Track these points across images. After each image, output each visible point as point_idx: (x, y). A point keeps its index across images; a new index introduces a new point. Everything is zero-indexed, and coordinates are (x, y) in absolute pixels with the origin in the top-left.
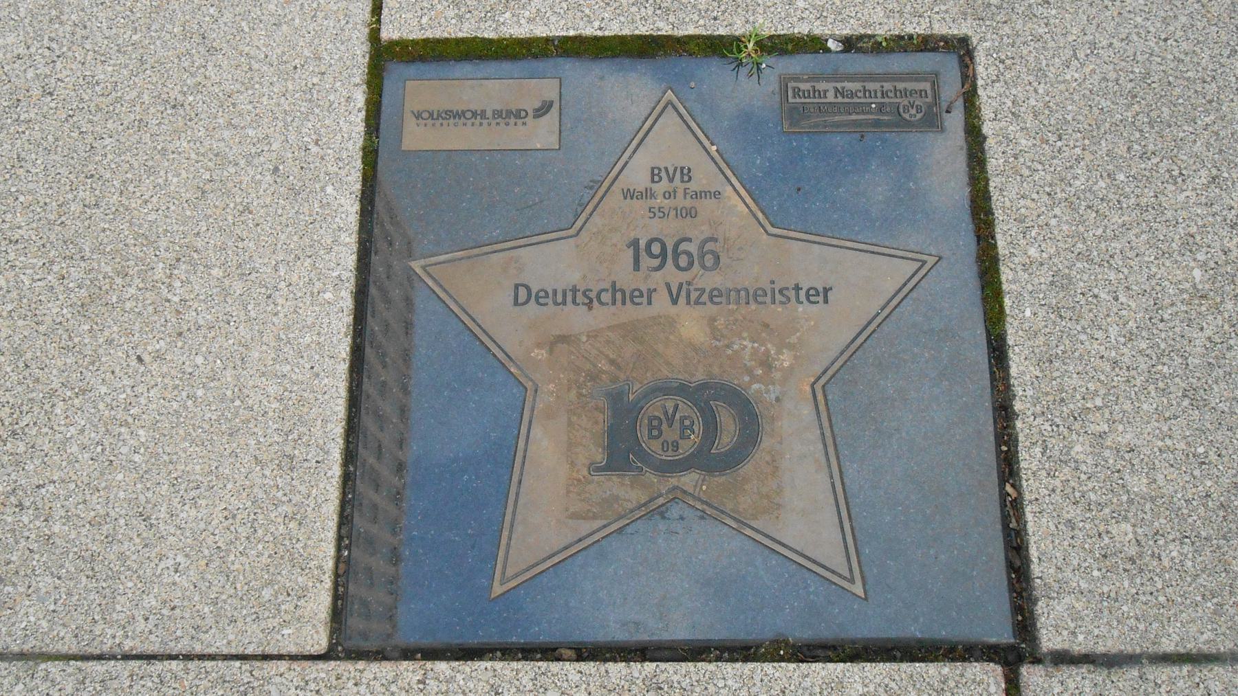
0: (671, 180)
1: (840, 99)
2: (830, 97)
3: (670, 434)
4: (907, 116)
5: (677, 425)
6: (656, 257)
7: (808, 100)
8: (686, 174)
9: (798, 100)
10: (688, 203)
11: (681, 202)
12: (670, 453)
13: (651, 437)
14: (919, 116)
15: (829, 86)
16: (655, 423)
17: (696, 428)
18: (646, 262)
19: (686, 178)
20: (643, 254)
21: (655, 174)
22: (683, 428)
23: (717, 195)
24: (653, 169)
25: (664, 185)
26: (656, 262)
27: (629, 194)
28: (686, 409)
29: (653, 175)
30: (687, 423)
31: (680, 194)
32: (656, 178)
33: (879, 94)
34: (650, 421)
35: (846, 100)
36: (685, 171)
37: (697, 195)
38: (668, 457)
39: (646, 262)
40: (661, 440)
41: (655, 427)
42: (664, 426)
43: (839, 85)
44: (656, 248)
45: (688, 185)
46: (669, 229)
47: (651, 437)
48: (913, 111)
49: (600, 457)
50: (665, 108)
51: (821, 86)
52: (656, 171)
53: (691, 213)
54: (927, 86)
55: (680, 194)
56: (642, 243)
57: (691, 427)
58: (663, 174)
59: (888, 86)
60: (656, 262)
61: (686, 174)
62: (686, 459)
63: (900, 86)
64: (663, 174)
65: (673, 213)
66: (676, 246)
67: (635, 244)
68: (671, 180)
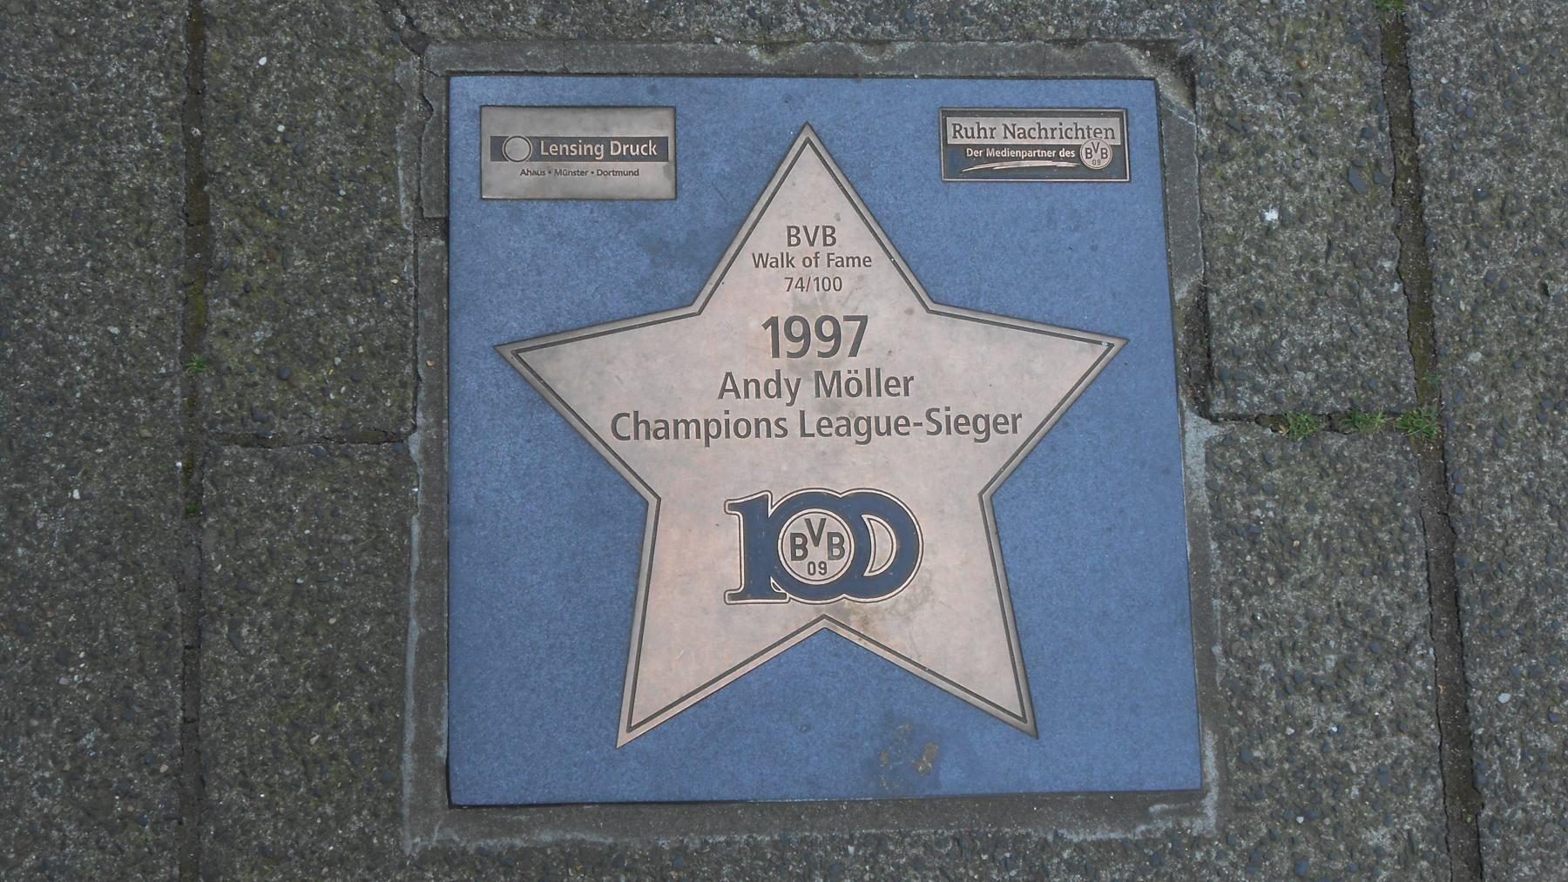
0: (812, 244)
1: (1010, 141)
3: (818, 553)
4: (1088, 163)
6: (796, 340)
9: (958, 141)
11: (822, 271)
12: (817, 576)
13: (794, 557)
14: (1104, 163)
15: (999, 123)
16: (799, 541)
17: (846, 546)
18: (786, 345)
21: (792, 232)
22: (831, 546)
23: (866, 262)
26: (799, 346)
27: (760, 260)
28: (835, 523)
29: (790, 236)
30: (836, 540)
31: (823, 260)
32: (794, 240)
33: (1057, 133)
34: (794, 536)
36: (829, 231)
38: (817, 579)
39: (786, 345)
40: (806, 561)
41: (799, 547)
42: (810, 545)
43: (1008, 121)
44: (797, 329)
47: (794, 557)
48: (1097, 156)
51: (986, 123)
52: (793, 232)
53: (835, 284)
54: (1114, 123)
55: (823, 260)
57: (840, 546)
58: (802, 235)
59: (1068, 123)
60: (799, 346)
61: (829, 234)
63: (1083, 122)
64: (802, 235)
66: (834, 351)
67: (773, 322)
68: (812, 244)
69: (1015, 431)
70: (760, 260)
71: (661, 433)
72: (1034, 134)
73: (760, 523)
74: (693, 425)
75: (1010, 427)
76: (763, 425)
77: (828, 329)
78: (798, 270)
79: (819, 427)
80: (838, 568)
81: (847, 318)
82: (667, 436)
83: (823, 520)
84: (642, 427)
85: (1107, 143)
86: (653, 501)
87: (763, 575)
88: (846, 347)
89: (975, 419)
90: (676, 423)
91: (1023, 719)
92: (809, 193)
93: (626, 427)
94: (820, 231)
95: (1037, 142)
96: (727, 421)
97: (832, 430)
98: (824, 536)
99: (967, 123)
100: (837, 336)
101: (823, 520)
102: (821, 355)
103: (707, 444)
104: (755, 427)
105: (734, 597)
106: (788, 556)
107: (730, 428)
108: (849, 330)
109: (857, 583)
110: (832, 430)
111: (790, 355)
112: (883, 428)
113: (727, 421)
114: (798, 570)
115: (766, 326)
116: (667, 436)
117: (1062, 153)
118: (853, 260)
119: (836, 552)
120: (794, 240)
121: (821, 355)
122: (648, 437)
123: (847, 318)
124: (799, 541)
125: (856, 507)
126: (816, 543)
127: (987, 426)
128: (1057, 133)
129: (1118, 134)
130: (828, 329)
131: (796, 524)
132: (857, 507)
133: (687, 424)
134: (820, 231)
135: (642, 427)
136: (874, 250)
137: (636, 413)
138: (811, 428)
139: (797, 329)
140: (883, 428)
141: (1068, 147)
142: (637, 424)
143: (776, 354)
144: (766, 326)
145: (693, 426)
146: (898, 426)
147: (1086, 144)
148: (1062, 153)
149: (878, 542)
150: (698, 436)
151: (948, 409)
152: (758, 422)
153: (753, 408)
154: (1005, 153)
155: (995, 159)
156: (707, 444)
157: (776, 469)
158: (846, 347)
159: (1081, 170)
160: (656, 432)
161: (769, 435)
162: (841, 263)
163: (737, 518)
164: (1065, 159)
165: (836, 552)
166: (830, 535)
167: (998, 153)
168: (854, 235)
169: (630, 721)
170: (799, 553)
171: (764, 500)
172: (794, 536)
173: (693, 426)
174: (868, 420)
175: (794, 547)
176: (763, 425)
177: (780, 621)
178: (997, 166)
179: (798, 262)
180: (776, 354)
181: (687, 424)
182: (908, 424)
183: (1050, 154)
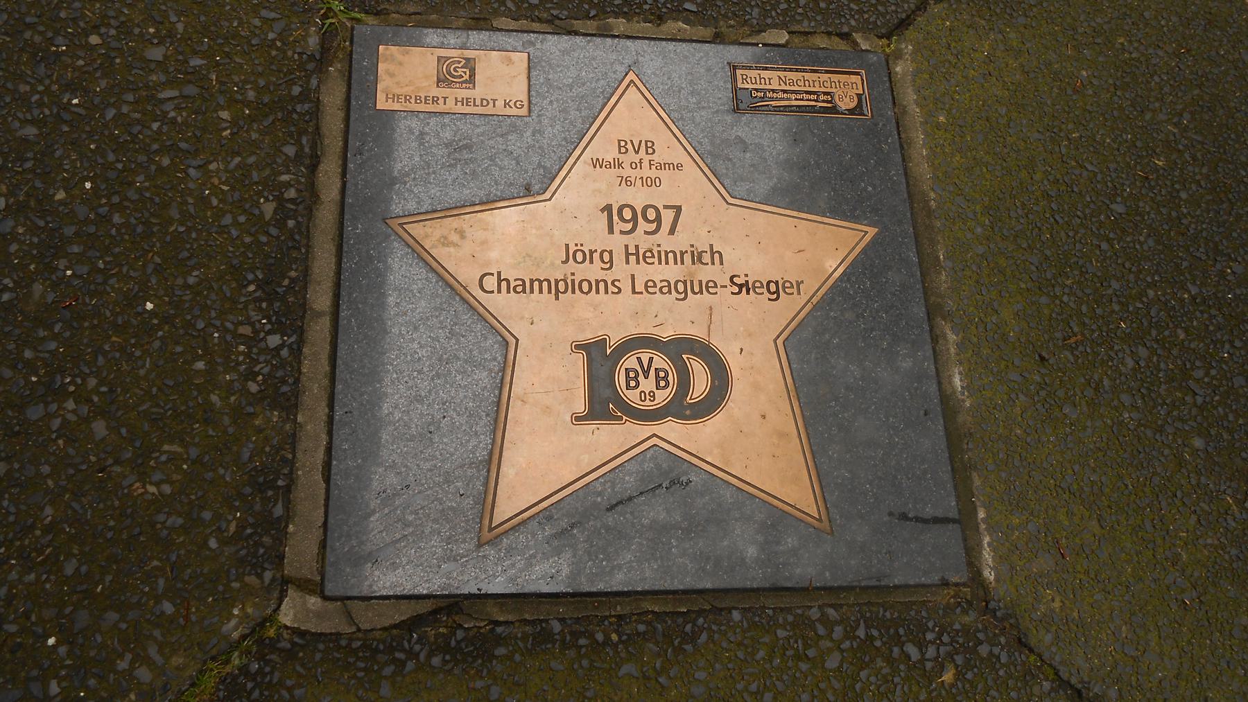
0: (637, 152)
3: (647, 384)
5: (652, 372)
7: (755, 86)
10: (653, 173)
11: (646, 172)
12: (648, 402)
17: (670, 378)
19: (650, 151)
20: (615, 218)
21: (622, 146)
23: (679, 167)
24: (619, 141)
25: (632, 156)
26: (629, 226)
27: (596, 163)
28: (660, 361)
29: (620, 146)
30: (662, 374)
31: (646, 164)
32: (623, 150)
33: (817, 84)
35: (788, 88)
36: (649, 144)
37: (661, 167)
38: (648, 405)
39: (619, 226)
41: (632, 379)
42: (641, 378)
43: (781, 74)
44: (627, 214)
45: (650, 157)
46: (638, 197)
49: (580, 407)
50: (628, 86)
52: (623, 144)
54: (854, 78)
55: (646, 164)
56: (615, 212)
57: (665, 378)
58: (629, 146)
60: (629, 226)
61: (650, 147)
63: (835, 77)
64: (629, 146)
65: (639, 182)
67: (608, 209)
68: (637, 152)
69: (799, 293)
70: (596, 163)
71: (519, 289)
73: (599, 358)
74: (545, 284)
75: (795, 290)
76: (602, 285)
77: (651, 214)
78: (627, 171)
79: (646, 287)
80: (663, 397)
81: (666, 207)
82: (524, 291)
83: (651, 359)
84: (504, 284)
85: (853, 93)
87: (603, 404)
88: (666, 226)
89: (769, 283)
90: (532, 281)
91: (820, 520)
92: (632, 116)
93: (491, 283)
94: (643, 144)
96: (573, 281)
97: (657, 290)
98: (653, 369)
99: (753, 74)
100: (658, 219)
101: (651, 359)
102: (646, 233)
103: (557, 298)
104: (595, 286)
105: (578, 419)
107: (574, 286)
108: (668, 216)
110: (657, 290)
111: (622, 232)
112: (697, 289)
113: (573, 281)
114: (632, 397)
115: (602, 210)
116: (524, 291)
117: (822, 97)
119: (662, 383)
120: (623, 150)
121: (646, 233)
122: (508, 292)
123: (666, 207)
124: (632, 375)
125: (679, 348)
126: (646, 374)
127: (775, 290)
128: (817, 84)
129: (860, 86)
130: (651, 214)
131: (630, 362)
132: (681, 348)
133: (541, 282)
134: (643, 144)
135: (504, 284)
136: (686, 160)
137: (499, 273)
138: (640, 287)
139: (627, 214)
140: (697, 289)
141: (825, 93)
142: (500, 281)
143: (611, 231)
144: (602, 210)
145: (545, 284)
146: (708, 287)
147: (837, 92)
148: (822, 97)
149: (697, 375)
150: (550, 292)
151: (746, 275)
152: (597, 282)
153: (593, 271)
154: (781, 95)
155: (772, 99)
156: (557, 298)
157: (614, 318)
158: (666, 226)
159: (834, 110)
161: (607, 292)
162: (661, 167)
163: (580, 359)
164: (823, 101)
168: (669, 148)
170: (633, 384)
171: (602, 343)
173: (545, 284)
174: (685, 283)
176: (602, 285)
177: (612, 440)
180: (611, 231)
181: (541, 282)
182: (716, 286)
183: (812, 97)
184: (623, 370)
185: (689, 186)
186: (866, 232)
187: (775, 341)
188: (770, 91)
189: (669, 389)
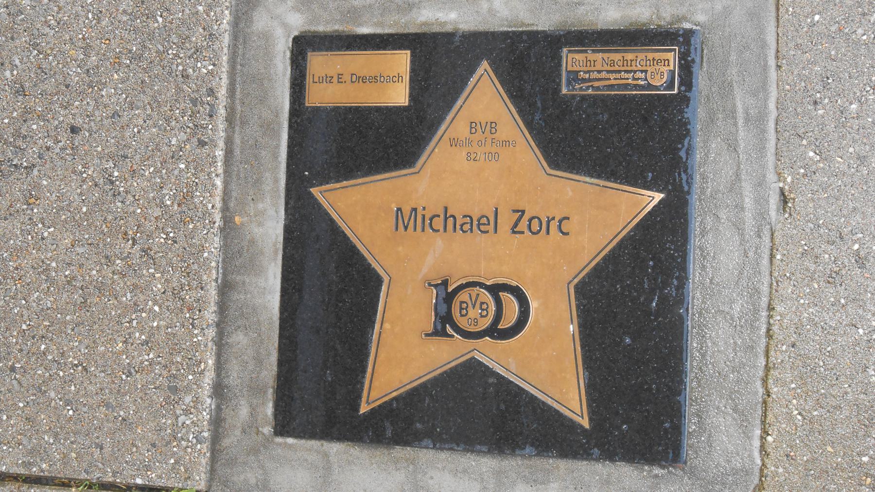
2: (599, 67)
8: (493, 126)
9: (575, 69)
25: (479, 135)
38: (472, 329)
40: (468, 317)
45: (493, 136)
47: (462, 316)
49: (430, 329)
54: (670, 56)
61: (493, 126)
62: (484, 331)
72: (620, 63)
86: (386, 279)
94: (489, 124)
95: (623, 69)
98: (478, 305)
105: (427, 335)
106: (458, 314)
109: (495, 332)
114: (462, 323)
118: (506, 143)
124: (464, 306)
126: (474, 307)
129: (672, 63)
131: (463, 296)
132: (495, 290)
160: (462, 226)
165: (485, 313)
166: (482, 303)
167: (599, 76)
169: (368, 400)
172: (462, 302)
175: (461, 309)
178: (596, 84)
179: (475, 144)
184: (458, 304)
185: (523, 153)
186: (653, 198)
187: (568, 284)
188: (593, 71)
189: (488, 317)
